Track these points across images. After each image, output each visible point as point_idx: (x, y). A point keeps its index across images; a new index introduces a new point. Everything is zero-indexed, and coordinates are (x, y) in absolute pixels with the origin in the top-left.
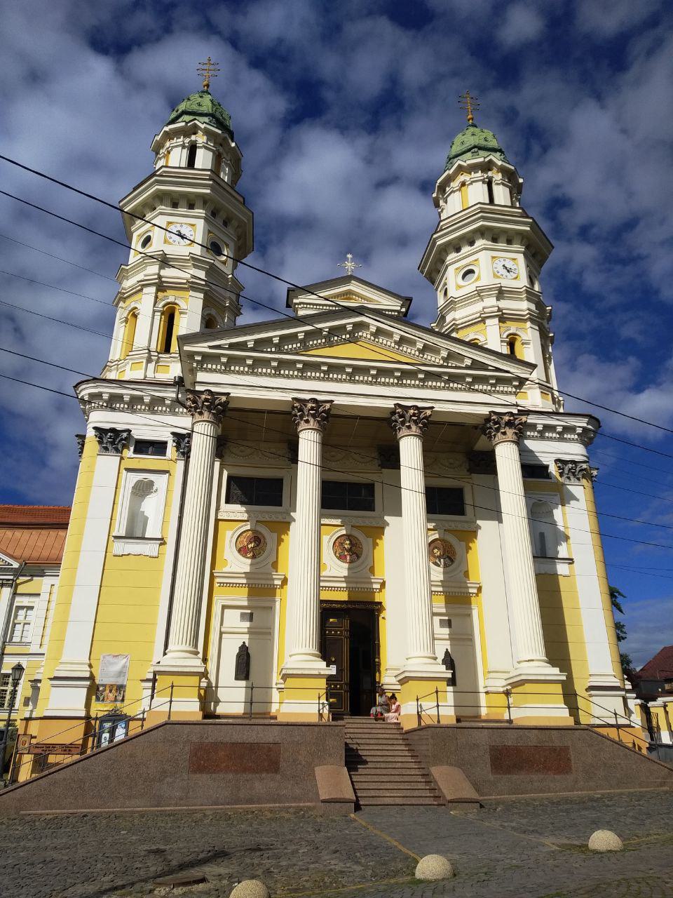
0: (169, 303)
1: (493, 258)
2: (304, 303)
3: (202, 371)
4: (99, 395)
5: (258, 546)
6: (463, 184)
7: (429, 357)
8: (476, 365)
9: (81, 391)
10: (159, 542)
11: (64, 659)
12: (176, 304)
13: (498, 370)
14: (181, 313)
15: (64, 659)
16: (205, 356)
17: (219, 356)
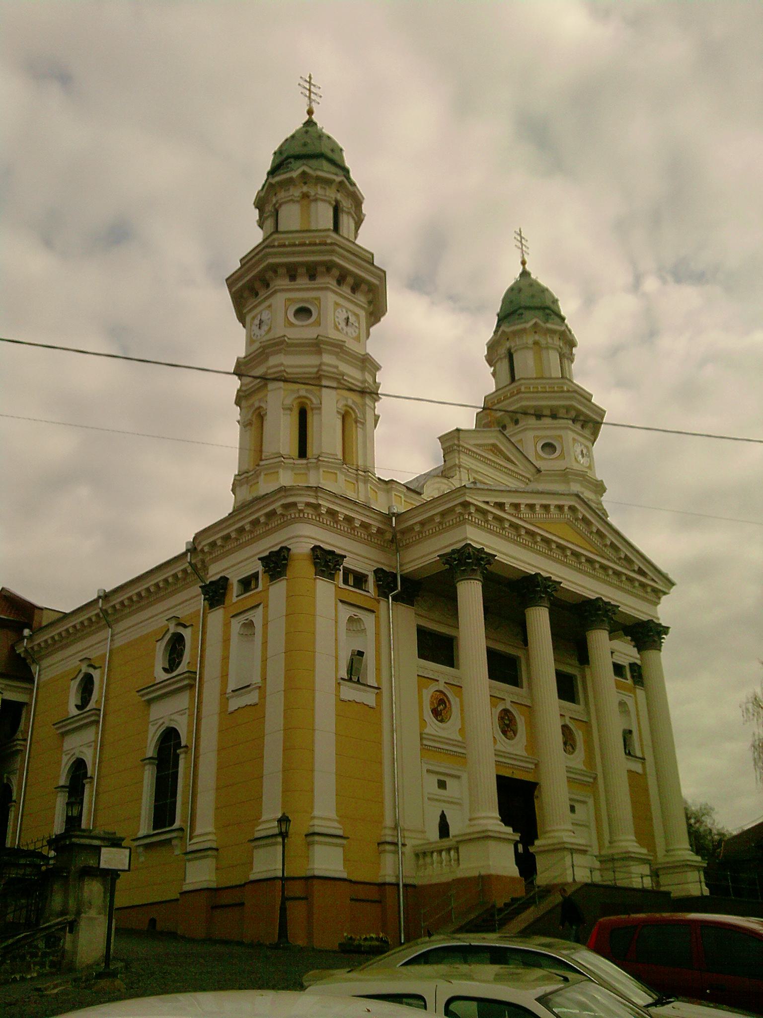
1: (574, 439)
2: (463, 447)
3: (471, 525)
4: (316, 507)
5: (444, 709)
6: (536, 343)
7: (609, 552)
8: (641, 572)
9: (291, 495)
10: (376, 691)
11: (316, 813)
12: (351, 408)
13: (653, 580)
14: (356, 422)
15: (316, 813)
16: (479, 510)
17: (484, 512)
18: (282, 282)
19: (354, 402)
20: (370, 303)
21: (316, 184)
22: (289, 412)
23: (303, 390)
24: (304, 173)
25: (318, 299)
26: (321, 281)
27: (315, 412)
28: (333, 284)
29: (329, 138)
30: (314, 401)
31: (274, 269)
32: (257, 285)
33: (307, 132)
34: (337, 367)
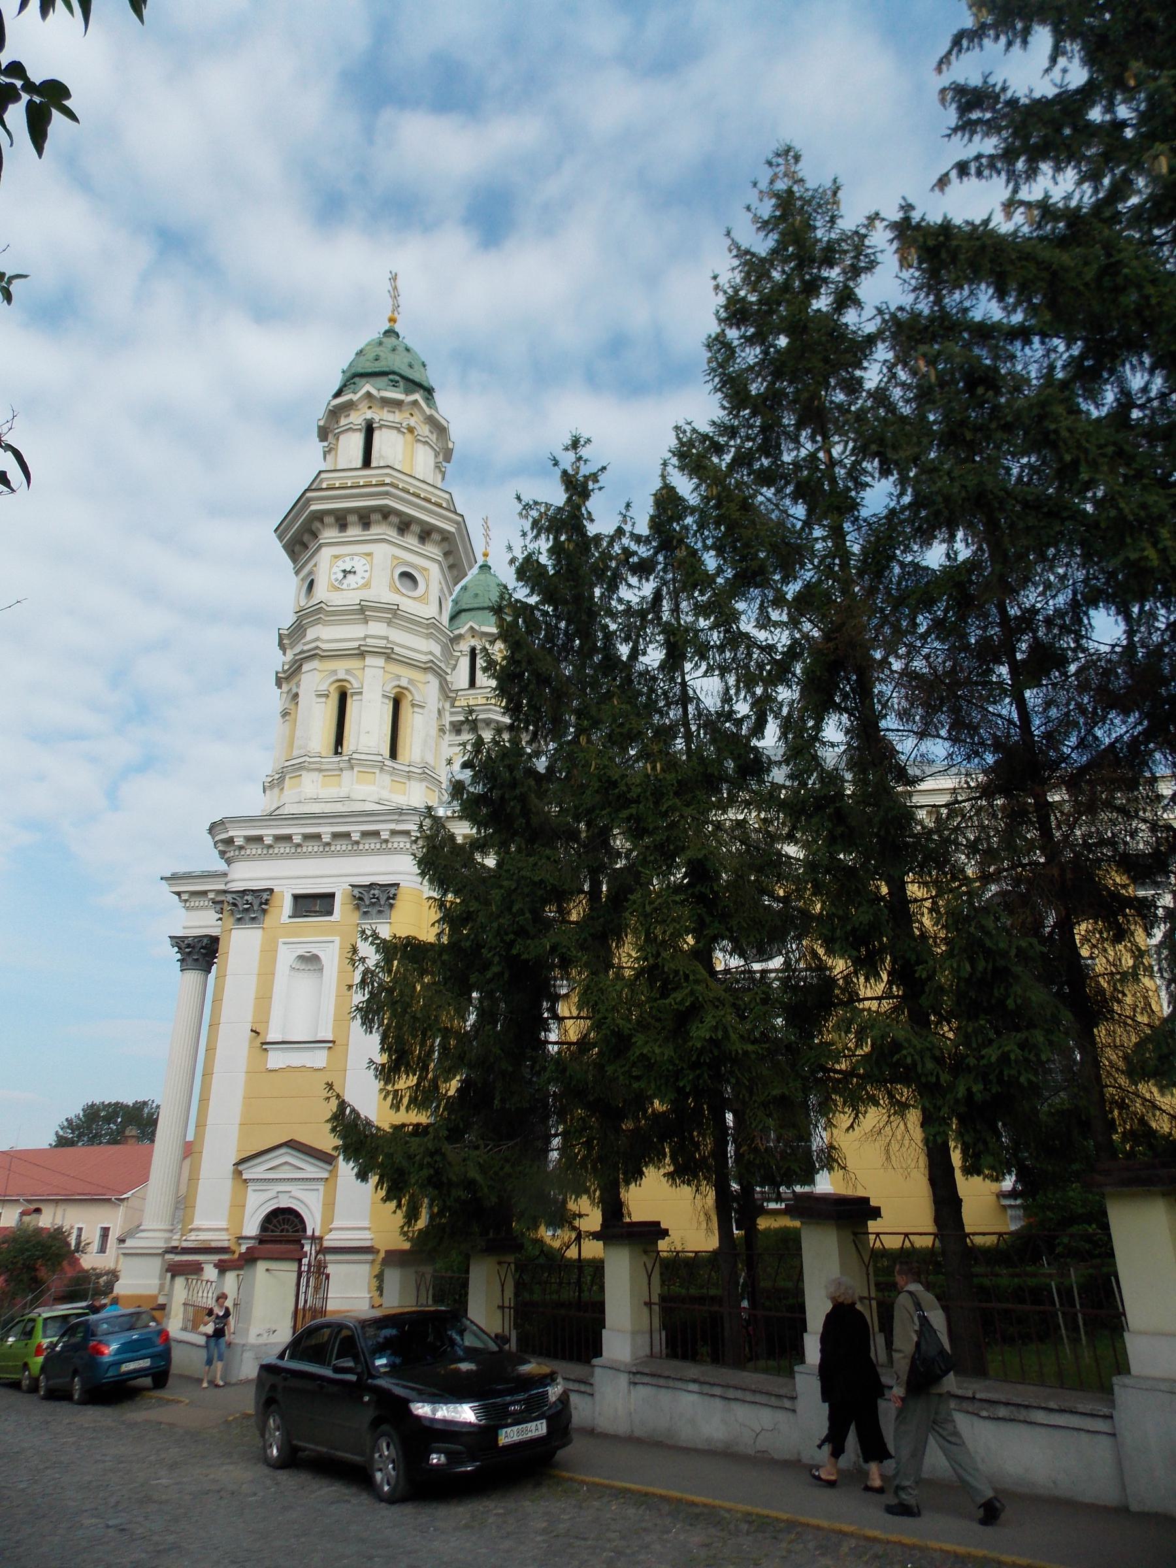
0: (399, 686)
12: (406, 689)
14: (413, 705)
18: (329, 534)
19: (411, 681)
20: (446, 554)
21: (383, 407)
22: (324, 699)
23: (341, 667)
24: (369, 395)
25: (369, 554)
26: (376, 530)
27: (355, 698)
28: (391, 533)
29: (408, 350)
30: (356, 686)
31: (319, 516)
32: (306, 538)
33: (380, 343)
34: (386, 638)
